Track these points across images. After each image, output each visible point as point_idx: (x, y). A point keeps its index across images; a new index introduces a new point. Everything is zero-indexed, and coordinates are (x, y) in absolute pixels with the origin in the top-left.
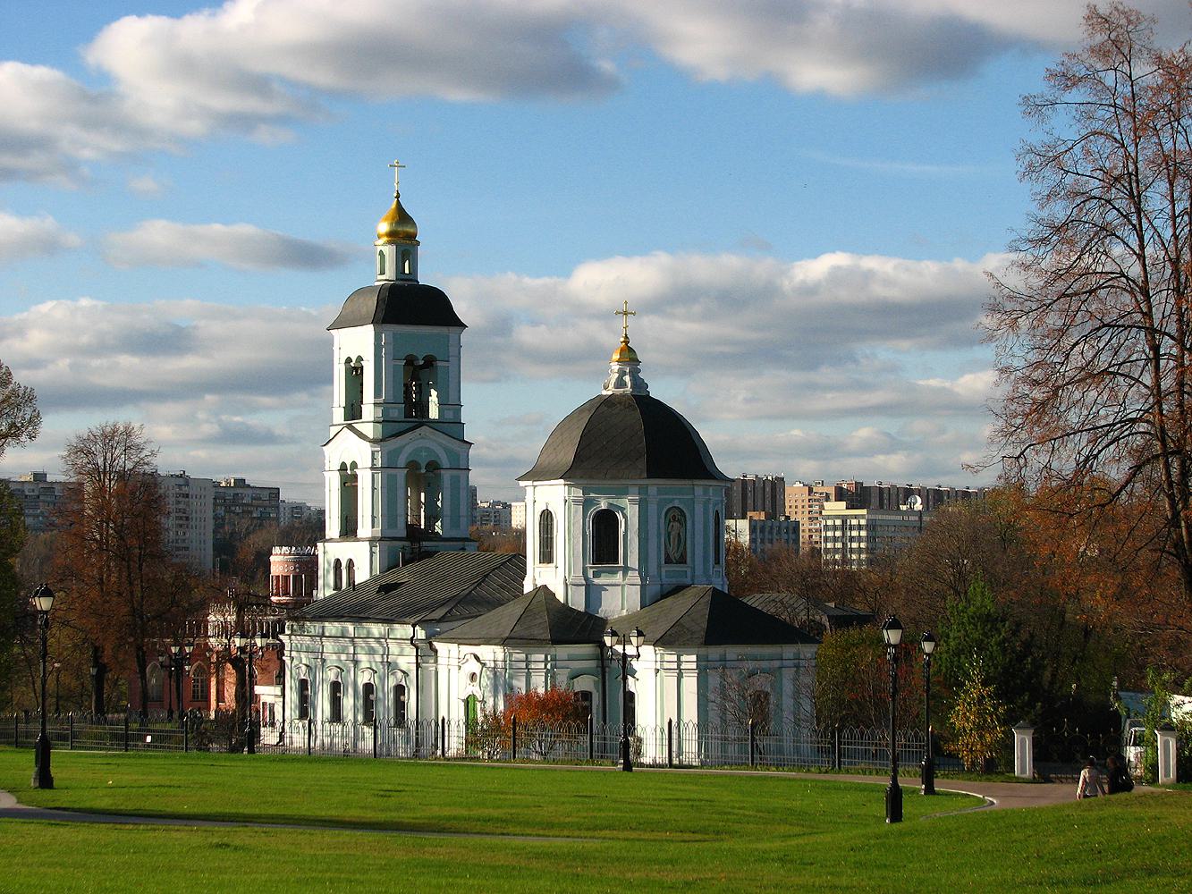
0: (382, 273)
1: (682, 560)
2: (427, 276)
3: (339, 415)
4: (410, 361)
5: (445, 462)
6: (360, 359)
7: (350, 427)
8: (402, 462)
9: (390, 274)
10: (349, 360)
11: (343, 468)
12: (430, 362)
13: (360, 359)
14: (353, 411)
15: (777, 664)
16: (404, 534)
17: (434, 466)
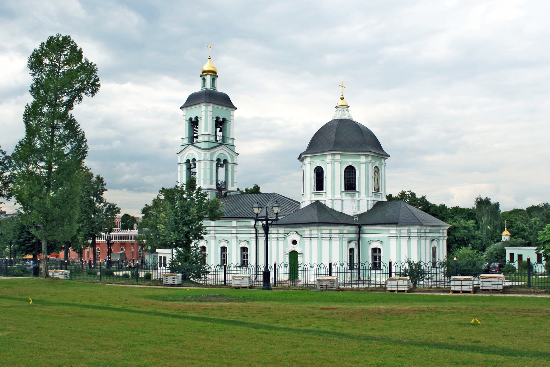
0: (204, 85)
1: (378, 190)
2: (220, 88)
3: (186, 142)
4: (217, 118)
5: (229, 161)
6: (197, 118)
7: (192, 145)
8: (215, 159)
9: (208, 86)
10: (191, 119)
11: (188, 161)
12: (224, 119)
13: (197, 118)
14: (192, 139)
15: (438, 235)
16: (214, 187)
17: (225, 161)
